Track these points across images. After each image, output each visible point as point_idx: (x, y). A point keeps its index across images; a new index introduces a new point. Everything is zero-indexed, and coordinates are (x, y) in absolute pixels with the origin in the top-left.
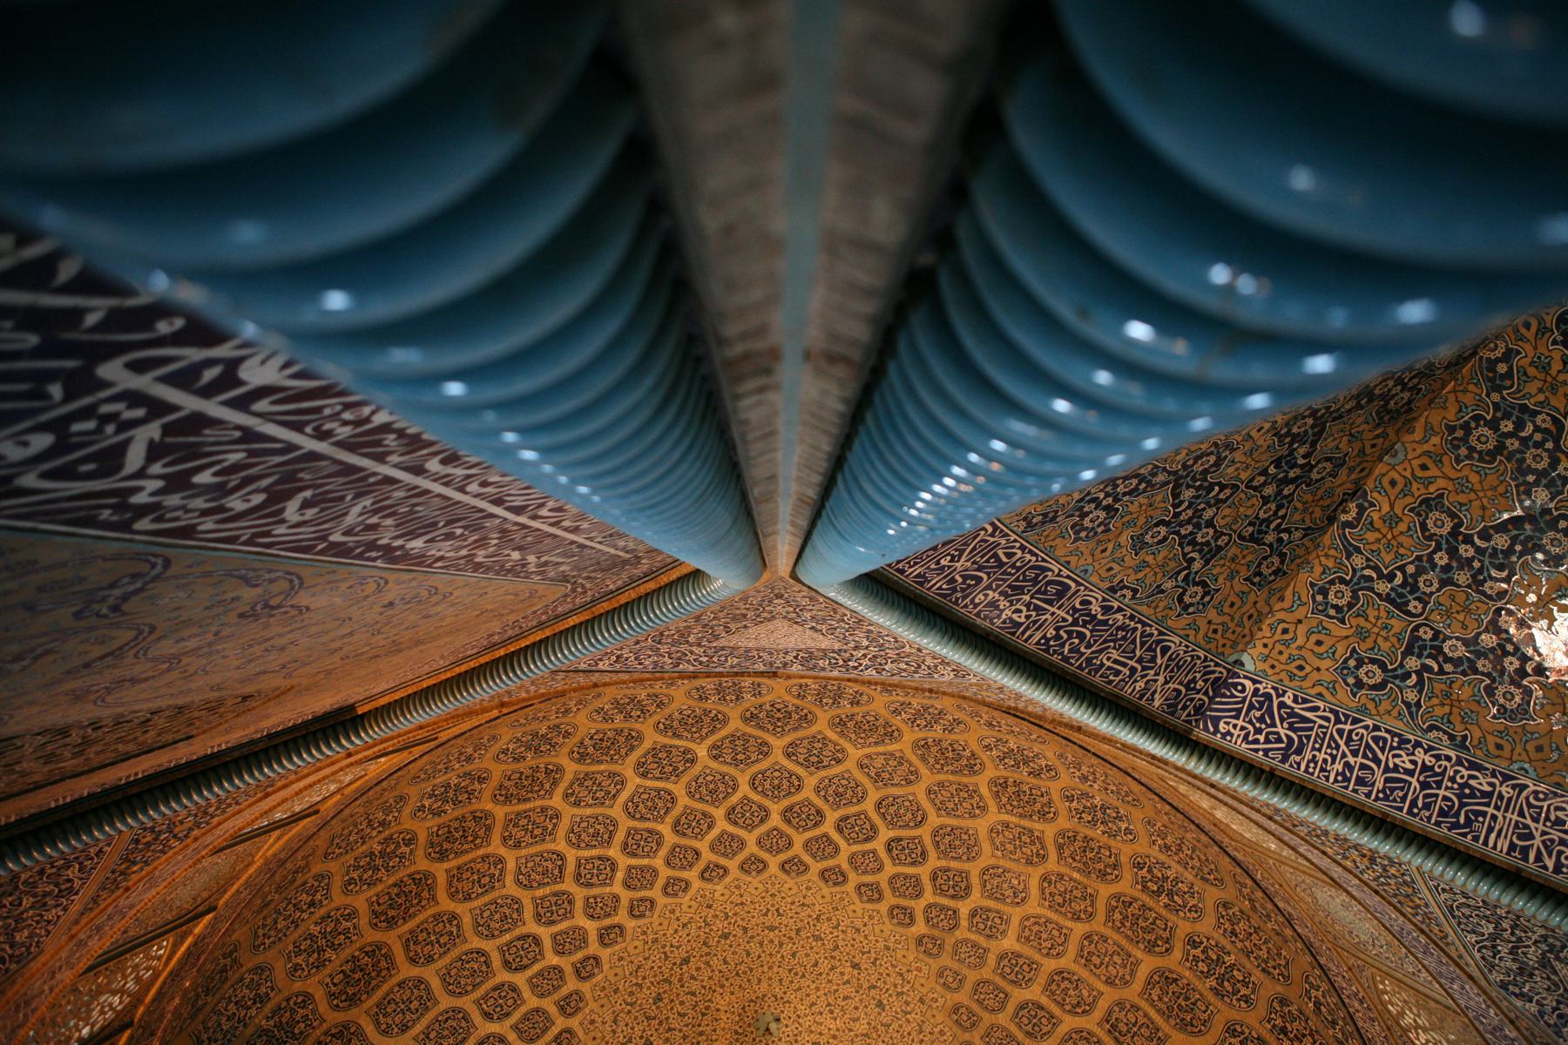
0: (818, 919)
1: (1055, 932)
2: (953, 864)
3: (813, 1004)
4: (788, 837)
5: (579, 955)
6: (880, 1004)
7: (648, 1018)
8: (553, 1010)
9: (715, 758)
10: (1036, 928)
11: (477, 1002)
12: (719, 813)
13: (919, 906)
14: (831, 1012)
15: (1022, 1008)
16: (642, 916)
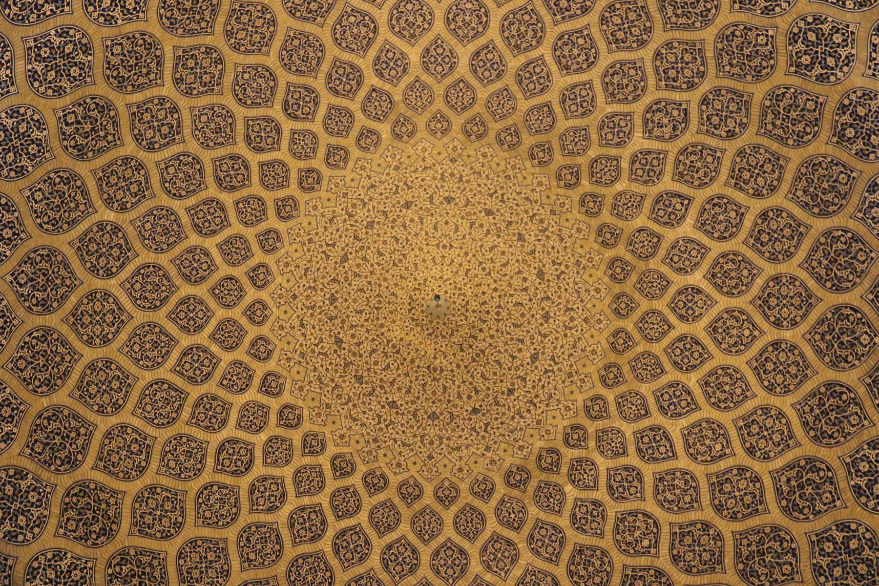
0: (351, 216)
2: (325, 67)
3: (433, 259)
4: (249, 197)
5: (273, 418)
6: (449, 200)
7: (370, 394)
8: (308, 460)
9: (123, 208)
10: (402, 21)
11: (251, 511)
12: (194, 239)
13: (361, 121)
14: (444, 247)
15: (475, 71)
16: (270, 353)
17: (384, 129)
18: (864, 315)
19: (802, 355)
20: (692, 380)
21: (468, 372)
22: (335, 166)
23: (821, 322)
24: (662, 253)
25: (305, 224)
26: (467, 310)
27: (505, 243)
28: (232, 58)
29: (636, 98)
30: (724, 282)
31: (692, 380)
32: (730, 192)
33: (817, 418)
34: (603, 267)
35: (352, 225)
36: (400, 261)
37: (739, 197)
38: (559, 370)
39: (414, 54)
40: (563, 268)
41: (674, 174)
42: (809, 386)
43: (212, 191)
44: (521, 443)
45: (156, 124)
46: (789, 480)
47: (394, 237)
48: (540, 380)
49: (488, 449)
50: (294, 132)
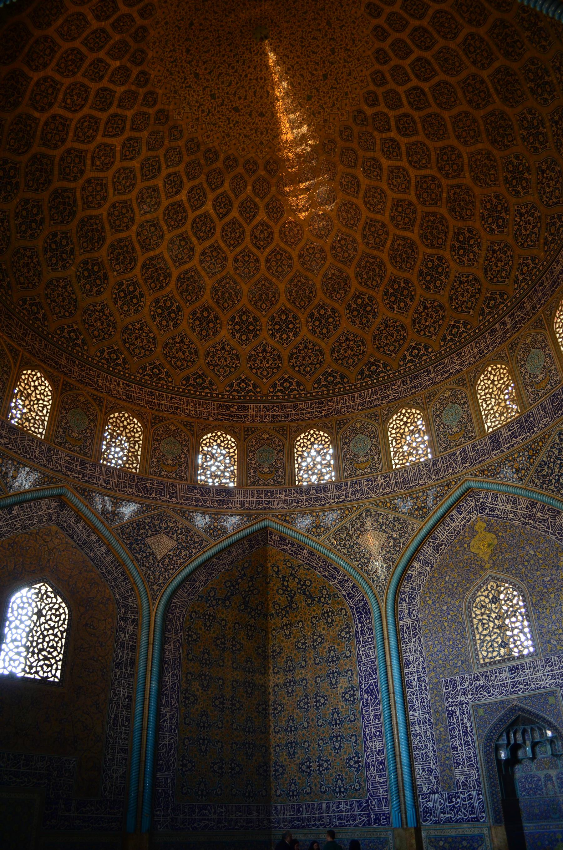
0: (346, 50)
1: (404, 186)
2: (419, 126)
3: (288, 57)
10: (402, 176)
15: (352, 176)
17: (369, 111)
18: (128, 272)
19: (122, 231)
20: (136, 164)
21: (215, 30)
22: (376, 73)
23: (133, 249)
24: (205, 186)
25: (364, 30)
26: (247, 49)
27: (266, 103)
28: (465, 107)
29: (281, 231)
30: (174, 209)
31: (136, 164)
32: (212, 241)
33: (91, 225)
34: (218, 148)
35: (341, 45)
36: (302, 42)
37: (207, 243)
38: (182, 87)
39: (385, 163)
40: (231, 125)
41: (236, 220)
42: (107, 227)
43: (425, 22)
44: (157, 44)
45: (478, 51)
46: (69, 198)
47: (316, 53)
48: (183, 72)
49: (166, 23)
50: (409, 80)
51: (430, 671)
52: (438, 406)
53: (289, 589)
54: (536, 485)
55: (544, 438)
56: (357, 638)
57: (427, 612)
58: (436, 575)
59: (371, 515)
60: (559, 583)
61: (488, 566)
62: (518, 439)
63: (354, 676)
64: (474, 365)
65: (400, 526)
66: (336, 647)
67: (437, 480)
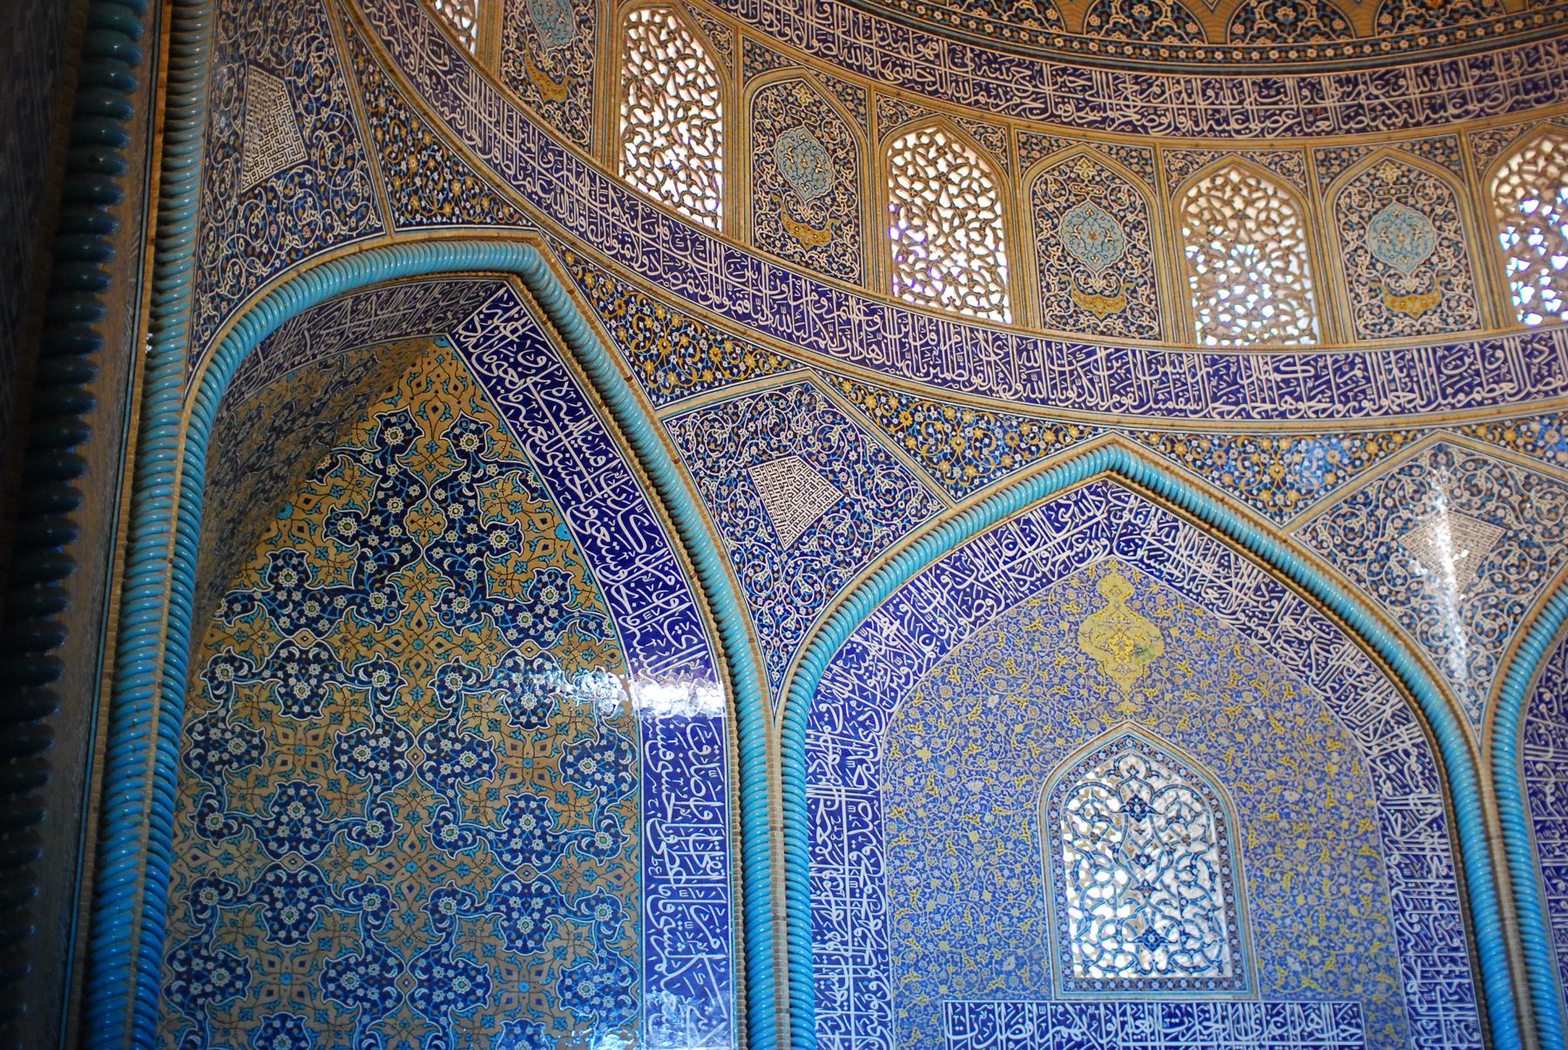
51: (905, 966)
52: (1053, 187)
53: (395, 531)
54: (1320, 545)
55: (1388, 438)
56: (649, 795)
57: (909, 781)
58: (955, 678)
59: (811, 408)
60: (1323, 818)
61: (1127, 707)
62: (1300, 405)
63: (626, 924)
64: (1189, 140)
65: (886, 484)
66: (550, 804)
67: (1028, 399)
